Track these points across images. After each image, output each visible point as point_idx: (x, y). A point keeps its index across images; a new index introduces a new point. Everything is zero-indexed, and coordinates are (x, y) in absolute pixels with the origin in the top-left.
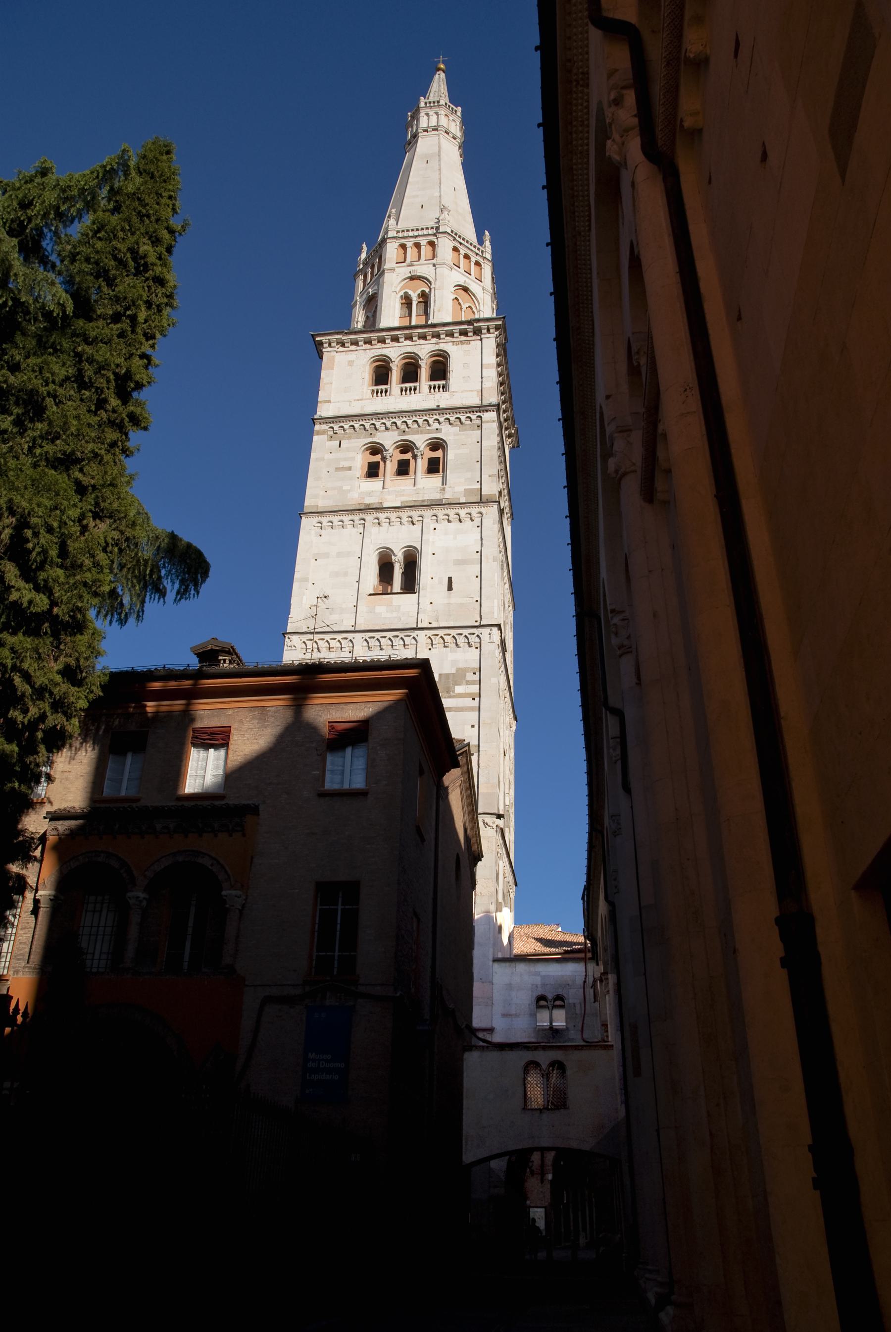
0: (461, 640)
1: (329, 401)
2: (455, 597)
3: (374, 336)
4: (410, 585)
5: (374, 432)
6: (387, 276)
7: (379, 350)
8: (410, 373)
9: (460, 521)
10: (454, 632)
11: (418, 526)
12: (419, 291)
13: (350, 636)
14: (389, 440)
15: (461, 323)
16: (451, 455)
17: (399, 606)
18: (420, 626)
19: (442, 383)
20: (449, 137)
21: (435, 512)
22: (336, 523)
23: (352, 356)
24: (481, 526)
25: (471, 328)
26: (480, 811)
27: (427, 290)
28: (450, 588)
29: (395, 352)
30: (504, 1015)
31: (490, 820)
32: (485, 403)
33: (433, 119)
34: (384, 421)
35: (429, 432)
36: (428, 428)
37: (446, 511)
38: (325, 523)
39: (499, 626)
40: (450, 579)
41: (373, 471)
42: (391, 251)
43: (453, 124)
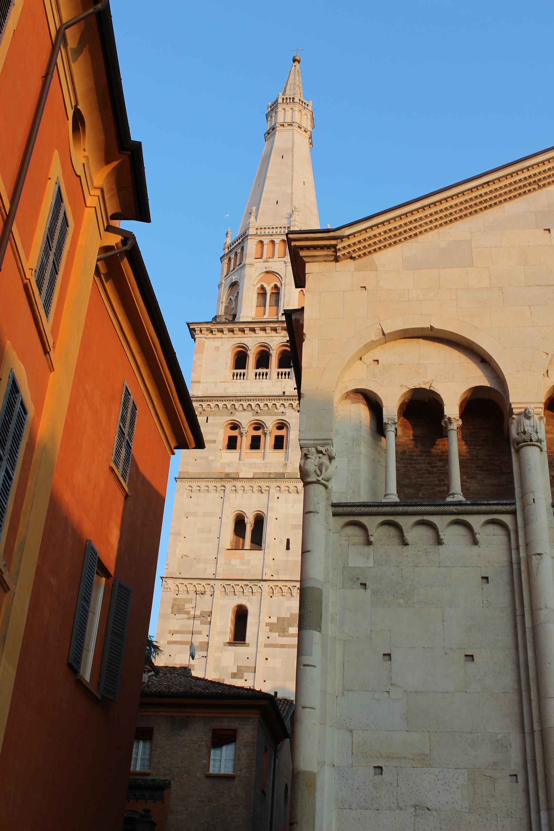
1: (199, 382)
3: (236, 327)
4: (258, 541)
5: (233, 411)
6: (248, 271)
8: (263, 360)
11: (265, 495)
12: (272, 285)
13: (212, 583)
14: (245, 420)
17: (249, 560)
18: (264, 578)
20: (302, 131)
21: (279, 484)
22: (203, 488)
23: (218, 343)
27: (279, 285)
28: (288, 548)
33: (289, 113)
34: (242, 403)
35: (276, 414)
36: (276, 411)
37: (287, 484)
38: (195, 488)
40: (288, 540)
41: (232, 444)
42: (251, 246)
43: (305, 117)
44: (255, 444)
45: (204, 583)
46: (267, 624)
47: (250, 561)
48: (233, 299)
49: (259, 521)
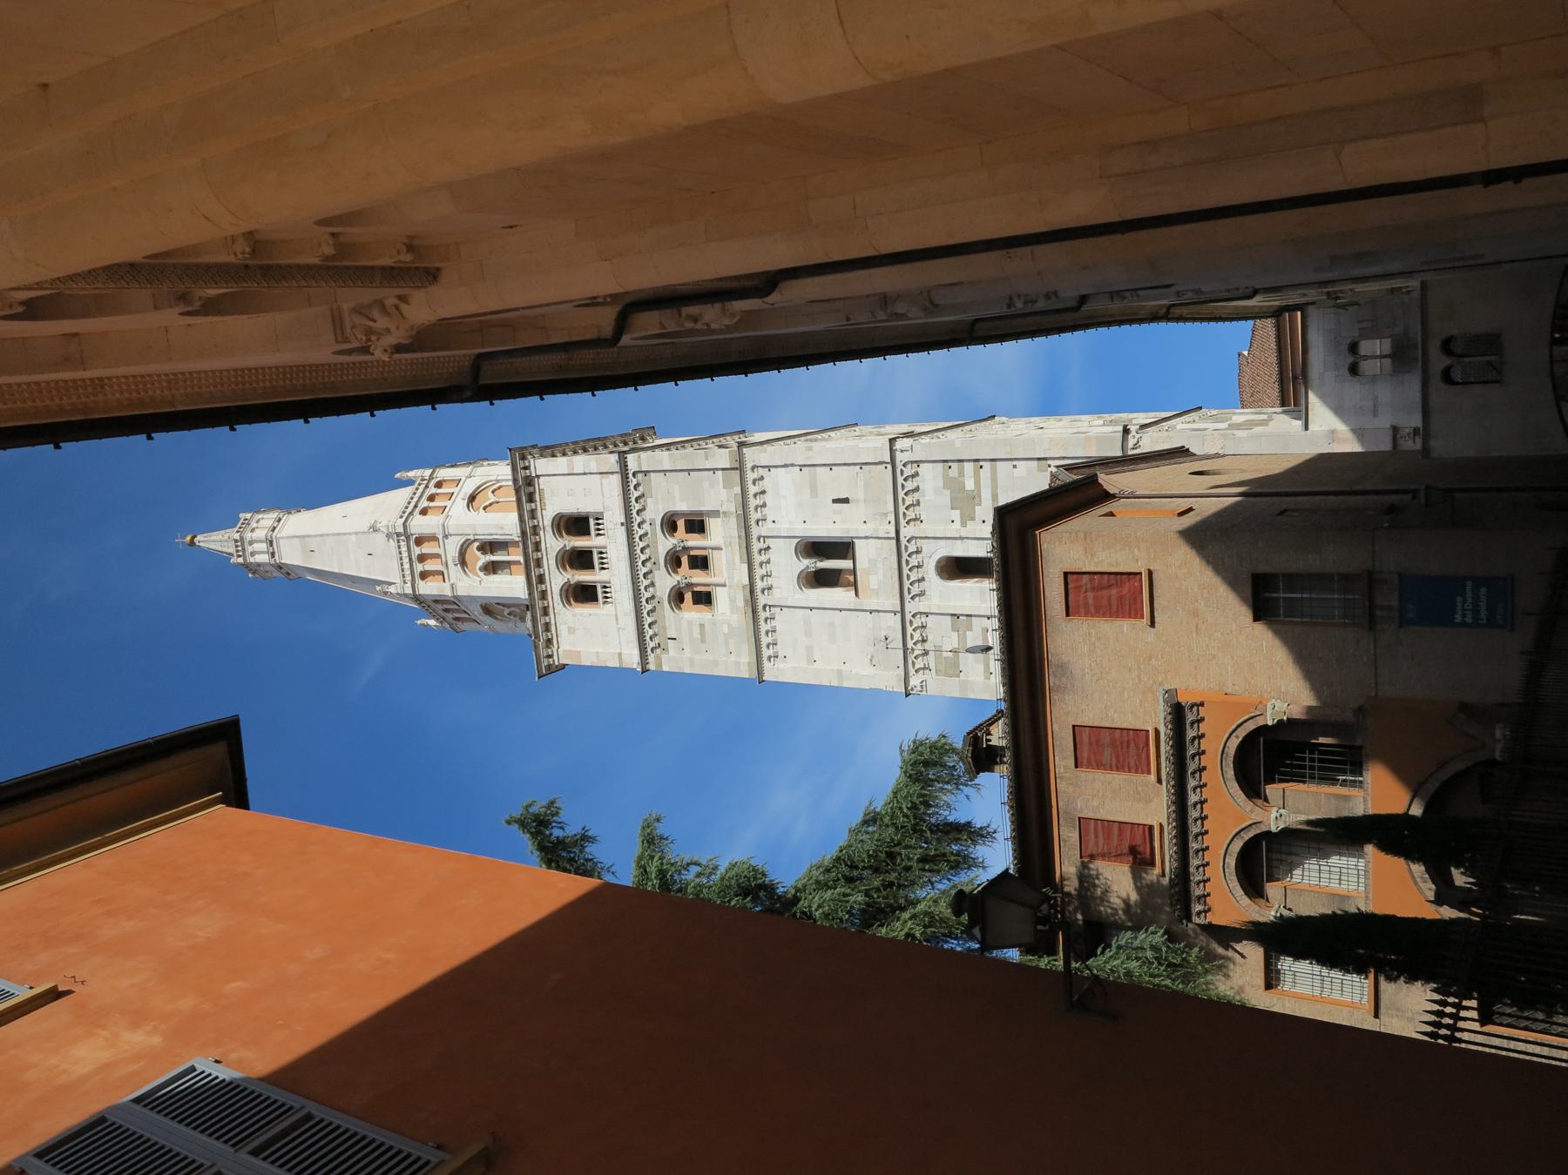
0: (910, 485)
2: (857, 494)
3: (539, 604)
4: (843, 548)
6: (461, 592)
7: (555, 599)
8: (581, 559)
9: (763, 492)
10: (901, 494)
11: (769, 542)
13: (908, 617)
14: (665, 582)
15: (519, 501)
16: (682, 507)
19: (592, 522)
21: (753, 522)
22: (770, 640)
23: (563, 630)
24: (769, 468)
25: (526, 489)
26: (1119, 454)
27: (476, 544)
28: (846, 501)
29: (557, 579)
30: (1375, 413)
31: (1131, 443)
32: (617, 468)
33: (257, 547)
38: (771, 652)
39: (892, 441)
40: (836, 501)
41: (704, 599)
42: (428, 588)
44: (701, 563)
45: (909, 630)
46: (964, 524)
47: (873, 560)
48: (507, 611)
49: (816, 548)
